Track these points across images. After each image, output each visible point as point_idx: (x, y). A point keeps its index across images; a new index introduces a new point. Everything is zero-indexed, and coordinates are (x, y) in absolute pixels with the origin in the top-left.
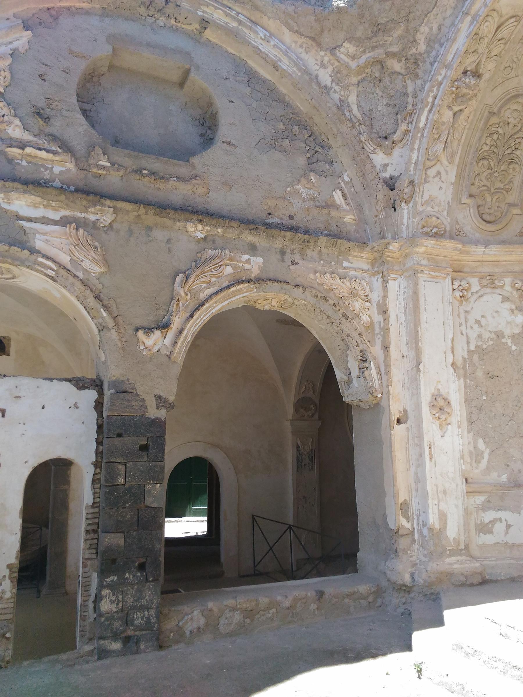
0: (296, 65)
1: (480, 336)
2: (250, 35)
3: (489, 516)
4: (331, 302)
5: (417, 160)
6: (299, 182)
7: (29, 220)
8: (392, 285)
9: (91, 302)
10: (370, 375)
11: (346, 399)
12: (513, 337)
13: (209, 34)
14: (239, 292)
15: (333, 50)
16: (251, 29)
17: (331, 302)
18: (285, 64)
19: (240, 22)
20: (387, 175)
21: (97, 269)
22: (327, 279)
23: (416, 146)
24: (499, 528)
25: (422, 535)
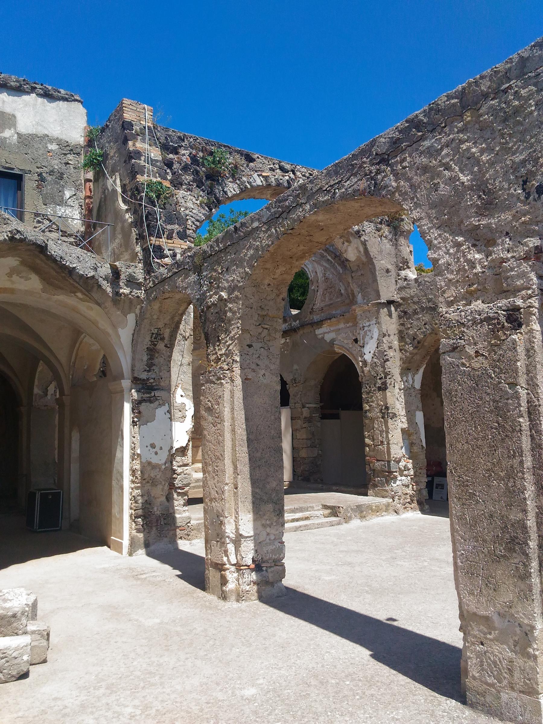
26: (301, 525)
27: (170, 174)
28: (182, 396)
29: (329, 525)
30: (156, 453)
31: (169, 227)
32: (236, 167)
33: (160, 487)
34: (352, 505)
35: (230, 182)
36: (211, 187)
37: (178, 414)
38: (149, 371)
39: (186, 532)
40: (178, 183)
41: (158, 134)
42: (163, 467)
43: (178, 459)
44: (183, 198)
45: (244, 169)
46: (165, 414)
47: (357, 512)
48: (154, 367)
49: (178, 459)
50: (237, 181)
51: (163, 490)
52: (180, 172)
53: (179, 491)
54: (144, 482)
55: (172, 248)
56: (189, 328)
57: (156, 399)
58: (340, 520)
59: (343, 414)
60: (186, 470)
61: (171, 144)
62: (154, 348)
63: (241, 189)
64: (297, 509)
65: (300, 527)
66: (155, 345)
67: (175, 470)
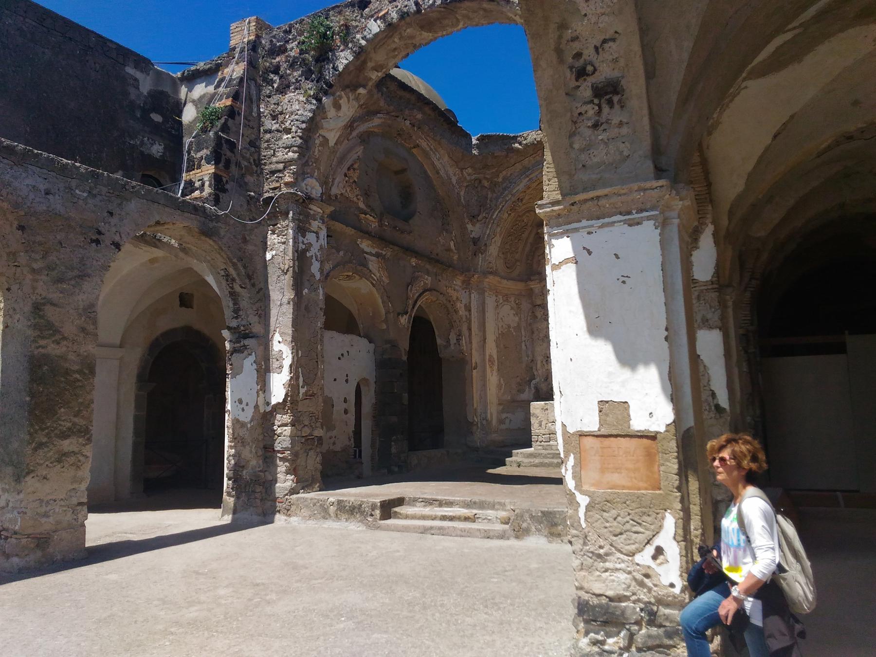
0: (447, 174)
1: (502, 326)
2: (432, 155)
3: (504, 416)
4: (452, 303)
5: (489, 234)
6: (440, 236)
7: (367, 253)
8: (472, 295)
9: (385, 298)
10: (462, 344)
11: (441, 356)
12: (514, 328)
13: (414, 151)
14: (426, 295)
15: (462, 169)
16: (434, 153)
17: (452, 303)
18: (442, 173)
19: (431, 149)
20: (472, 236)
21: (386, 281)
22: (449, 290)
23: (490, 226)
24: (507, 421)
25: (482, 424)
26: (433, 525)
27: (278, 81)
28: (279, 342)
29: (483, 535)
30: (243, 410)
31: (199, 155)
32: (347, 27)
33: (248, 448)
34: (533, 510)
35: (341, 51)
36: (320, 72)
37: (274, 364)
38: (237, 318)
39: (285, 505)
40: (284, 86)
41: (263, 42)
42: (249, 426)
43: (278, 416)
44: (289, 102)
45: (357, 23)
46: (252, 365)
47: (540, 523)
48: (241, 313)
49: (278, 416)
50: (350, 45)
51: (251, 452)
52: (288, 72)
53: (279, 455)
54: (236, 441)
55: (201, 178)
56: (288, 258)
57: (245, 347)
58: (504, 531)
59: (853, 341)
60: (285, 430)
61: (278, 44)
62: (234, 292)
63: (355, 52)
64: (475, 503)
65: (431, 528)
66: (232, 288)
67: (275, 431)
